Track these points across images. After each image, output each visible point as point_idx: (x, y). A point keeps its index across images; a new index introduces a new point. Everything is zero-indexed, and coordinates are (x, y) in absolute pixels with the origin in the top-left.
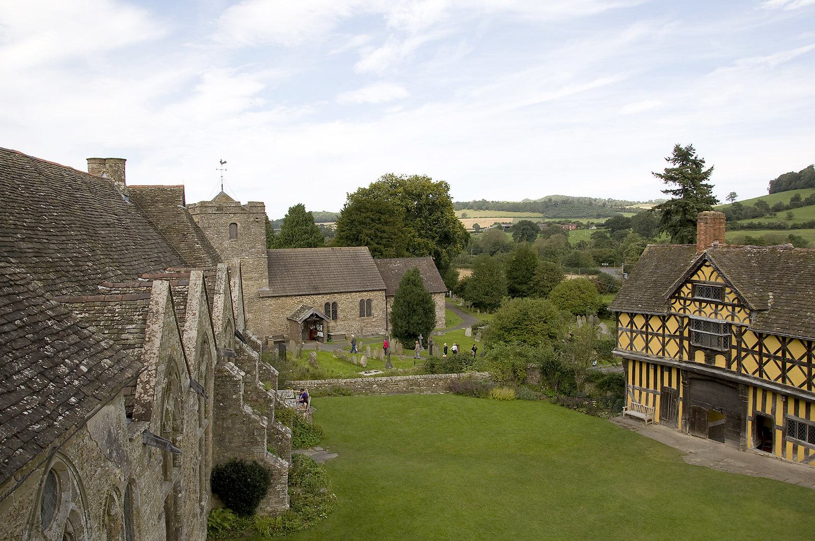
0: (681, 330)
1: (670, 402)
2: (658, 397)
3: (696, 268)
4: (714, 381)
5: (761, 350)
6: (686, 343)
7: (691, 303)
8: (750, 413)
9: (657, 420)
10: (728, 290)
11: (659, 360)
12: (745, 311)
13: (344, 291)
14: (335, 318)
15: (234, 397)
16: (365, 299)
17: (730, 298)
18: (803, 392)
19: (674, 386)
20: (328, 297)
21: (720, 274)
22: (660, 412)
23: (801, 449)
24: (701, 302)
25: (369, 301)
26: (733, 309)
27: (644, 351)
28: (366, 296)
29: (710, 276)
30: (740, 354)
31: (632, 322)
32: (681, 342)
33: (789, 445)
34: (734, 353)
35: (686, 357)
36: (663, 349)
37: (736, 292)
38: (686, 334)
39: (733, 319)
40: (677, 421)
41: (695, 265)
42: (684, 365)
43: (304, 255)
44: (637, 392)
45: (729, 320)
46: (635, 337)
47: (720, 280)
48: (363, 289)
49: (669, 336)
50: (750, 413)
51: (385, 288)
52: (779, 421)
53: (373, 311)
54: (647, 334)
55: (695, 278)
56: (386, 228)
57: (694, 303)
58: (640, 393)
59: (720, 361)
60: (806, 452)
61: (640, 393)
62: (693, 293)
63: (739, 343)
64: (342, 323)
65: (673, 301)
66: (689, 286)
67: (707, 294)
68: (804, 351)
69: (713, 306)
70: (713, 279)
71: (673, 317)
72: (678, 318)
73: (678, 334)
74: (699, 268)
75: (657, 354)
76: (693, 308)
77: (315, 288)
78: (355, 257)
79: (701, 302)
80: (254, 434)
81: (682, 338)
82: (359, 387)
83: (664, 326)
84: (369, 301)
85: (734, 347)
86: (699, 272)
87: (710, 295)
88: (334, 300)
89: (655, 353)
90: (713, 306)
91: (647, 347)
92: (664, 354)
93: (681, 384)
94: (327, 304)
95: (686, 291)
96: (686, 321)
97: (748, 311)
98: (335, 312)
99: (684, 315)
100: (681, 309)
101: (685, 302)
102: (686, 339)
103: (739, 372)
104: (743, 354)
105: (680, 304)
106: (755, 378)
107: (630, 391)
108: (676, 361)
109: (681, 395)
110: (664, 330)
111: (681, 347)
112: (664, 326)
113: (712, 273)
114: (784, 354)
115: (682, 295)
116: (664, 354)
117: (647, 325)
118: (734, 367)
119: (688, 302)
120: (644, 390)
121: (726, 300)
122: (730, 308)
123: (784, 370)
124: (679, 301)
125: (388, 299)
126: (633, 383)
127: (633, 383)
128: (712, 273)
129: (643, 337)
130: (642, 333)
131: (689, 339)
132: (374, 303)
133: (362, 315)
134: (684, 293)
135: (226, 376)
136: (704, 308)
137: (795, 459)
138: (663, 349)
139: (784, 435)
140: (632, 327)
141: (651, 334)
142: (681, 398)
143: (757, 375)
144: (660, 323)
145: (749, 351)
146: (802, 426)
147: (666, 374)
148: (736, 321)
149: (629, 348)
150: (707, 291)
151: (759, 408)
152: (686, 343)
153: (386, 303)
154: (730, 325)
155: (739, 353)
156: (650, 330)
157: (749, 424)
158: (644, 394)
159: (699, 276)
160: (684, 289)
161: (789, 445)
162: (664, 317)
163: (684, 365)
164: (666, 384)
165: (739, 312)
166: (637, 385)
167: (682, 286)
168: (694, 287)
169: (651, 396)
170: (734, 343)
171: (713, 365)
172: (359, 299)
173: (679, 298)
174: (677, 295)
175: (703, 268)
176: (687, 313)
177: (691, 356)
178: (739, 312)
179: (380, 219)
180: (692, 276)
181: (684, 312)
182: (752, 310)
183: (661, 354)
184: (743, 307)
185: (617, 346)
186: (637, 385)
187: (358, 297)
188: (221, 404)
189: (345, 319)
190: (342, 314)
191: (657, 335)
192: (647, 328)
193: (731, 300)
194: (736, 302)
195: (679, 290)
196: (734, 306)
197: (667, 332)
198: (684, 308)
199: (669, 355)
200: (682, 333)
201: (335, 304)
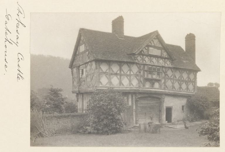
47: (160, 46)
59: (157, 85)
100: (141, 60)
105: (141, 57)
118: (163, 86)
124: (140, 56)
152: (142, 79)
155: (165, 81)
156: (122, 73)
159: (151, 43)
163: (141, 89)
181: (143, 62)
192: (120, 72)
194: (166, 56)
196: (165, 58)
198: (143, 60)
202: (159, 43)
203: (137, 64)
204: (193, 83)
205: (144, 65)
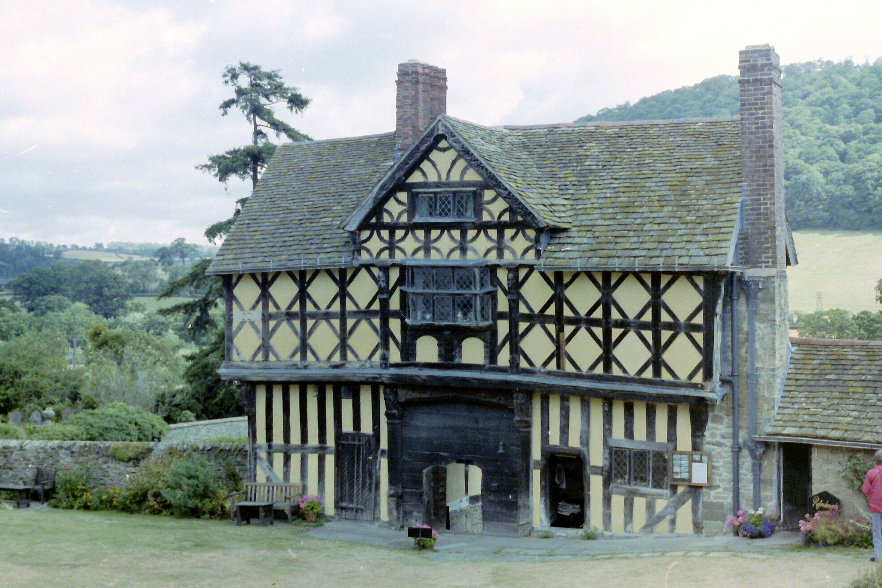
0: (385, 296)
1: (358, 467)
2: (330, 460)
3: (419, 155)
4: (453, 402)
5: (559, 310)
6: (395, 325)
7: (406, 235)
8: (536, 454)
9: (330, 509)
10: (489, 195)
11: (335, 371)
12: (524, 235)
17: (495, 209)
18: (644, 382)
19: (367, 427)
21: (474, 162)
22: (336, 492)
23: (640, 503)
24: (428, 228)
26: (501, 235)
27: (298, 357)
29: (449, 171)
30: (517, 326)
31: (265, 296)
32: (385, 323)
33: (618, 501)
34: (503, 327)
35: (395, 356)
36: (343, 346)
37: (509, 197)
38: (395, 303)
39: (500, 255)
40: (376, 505)
41: (417, 148)
42: (393, 371)
44: (278, 458)
45: (493, 258)
46: (274, 330)
47: (472, 176)
49: (354, 314)
50: (536, 454)
52: (597, 457)
54: (303, 317)
55: (416, 177)
57: (414, 235)
58: (287, 459)
60: (650, 507)
61: (287, 459)
62: (412, 210)
63: (514, 305)
65: (365, 234)
66: (403, 196)
67: (443, 210)
68: (646, 297)
69: (456, 234)
70: (455, 177)
71: (363, 272)
72: (376, 271)
73: (376, 306)
74: (425, 156)
75: (330, 358)
76: (410, 244)
79: (428, 228)
81: (385, 314)
83: (343, 294)
85: (502, 316)
86: (425, 165)
87: (449, 210)
89: (323, 355)
90: (456, 234)
91: (304, 347)
92: (344, 356)
93: (383, 420)
95: (395, 209)
96: (394, 275)
97: (531, 233)
99: (390, 262)
101: (392, 234)
102: (395, 314)
103: (514, 366)
104: (523, 326)
106: (549, 373)
107: (261, 459)
108: (372, 367)
109: (384, 445)
110: (343, 304)
111: (386, 335)
112: (343, 294)
113: (454, 163)
114: (607, 313)
115: (386, 219)
116: (344, 356)
117: (303, 296)
119: (399, 234)
120: (296, 449)
121: (486, 218)
122: (493, 233)
123: (607, 345)
124: (379, 235)
126: (269, 438)
127: (269, 438)
128: (454, 163)
129: (293, 327)
130: (290, 316)
131: (402, 313)
134: (390, 214)
136: (436, 240)
137: (629, 527)
138: (343, 346)
139: (607, 483)
140: (265, 306)
141: (313, 316)
142: (383, 452)
143: (552, 366)
144: (335, 289)
145: (536, 318)
146: (641, 456)
147: (347, 405)
148: (508, 257)
149: (260, 357)
150: (443, 202)
151: (555, 439)
152: (395, 325)
154: (493, 268)
155: (513, 327)
156: (310, 308)
157: (536, 475)
158: (296, 458)
159: (424, 174)
160: (392, 206)
161: (618, 501)
162: (343, 272)
163: (393, 371)
164: (347, 427)
165: (513, 238)
166: (278, 439)
167: (385, 199)
168: (413, 197)
169: (313, 460)
170: (503, 305)
171: (457, 361)
173: (380, 226)
174: (374, 220)
175: (435, 155)
176: (399, 256)
177: (408, 351)
178: (513, 238)
180: (409, 173)
181: (392, 255)
182: (540, 231)
183: (337, 359)
184: (520, 226)
185: (230, 360)
186: (278, 439)
191: (327, 316)
192: (303, 305)
193: (496, 215)
194: (506, 218)
195: (378, 208)
196: (500, 227)
197: (350, 307)
198: (391, 247)
199: (357, 356)
200: (385, 303)
202: (461, 164)
203: (368, 267)
204: (699, 337)
205: (403, 268)
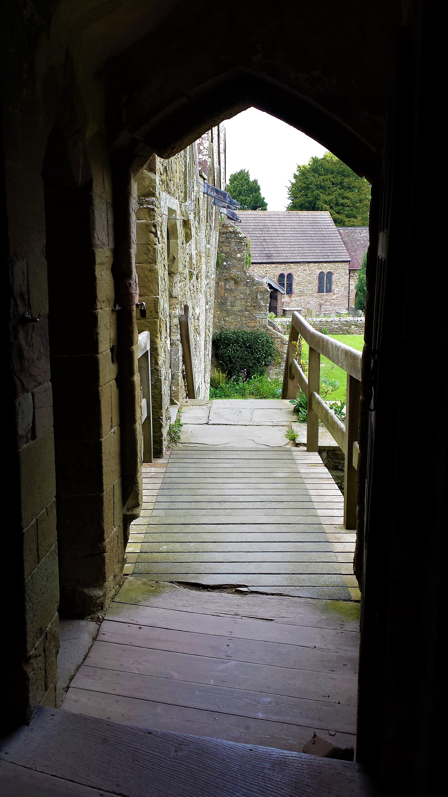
13: (301, 260)
14: (290, 292)
15: (239, 255)
16: (326, 271)
20: (283, 266)
25: (330, 274)
28: (326, 268)
43: (255, 219)
48: (324, 260)
51: (348, 259)
53: (333, 287)
56: (349, 195)
64: (298, 298)
77: (269, 256)
78: (314, 222)
80: (257, 297)
82: (336, 326)
84: (330, 274)
88: (289, 272)
94: (282, 276)
98: (290, 286)
125: (352, 274)
132: (335, 277)
133: (320, 290)
135: (231, 232)
153: (349, 278)
172: (318, 272)
179: (341, 183)
187: (316, 270)
188: (225, 263)
189: (302, 294)
190: (297, 288)
201: (290, 276)
